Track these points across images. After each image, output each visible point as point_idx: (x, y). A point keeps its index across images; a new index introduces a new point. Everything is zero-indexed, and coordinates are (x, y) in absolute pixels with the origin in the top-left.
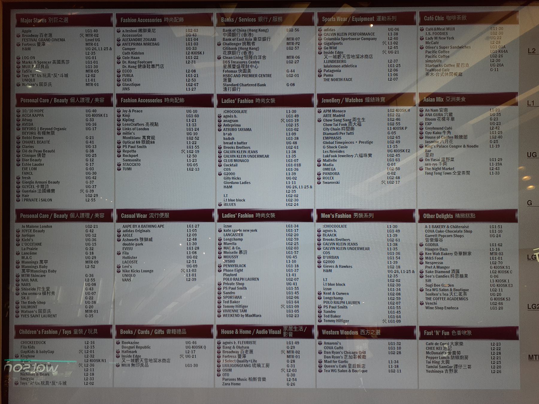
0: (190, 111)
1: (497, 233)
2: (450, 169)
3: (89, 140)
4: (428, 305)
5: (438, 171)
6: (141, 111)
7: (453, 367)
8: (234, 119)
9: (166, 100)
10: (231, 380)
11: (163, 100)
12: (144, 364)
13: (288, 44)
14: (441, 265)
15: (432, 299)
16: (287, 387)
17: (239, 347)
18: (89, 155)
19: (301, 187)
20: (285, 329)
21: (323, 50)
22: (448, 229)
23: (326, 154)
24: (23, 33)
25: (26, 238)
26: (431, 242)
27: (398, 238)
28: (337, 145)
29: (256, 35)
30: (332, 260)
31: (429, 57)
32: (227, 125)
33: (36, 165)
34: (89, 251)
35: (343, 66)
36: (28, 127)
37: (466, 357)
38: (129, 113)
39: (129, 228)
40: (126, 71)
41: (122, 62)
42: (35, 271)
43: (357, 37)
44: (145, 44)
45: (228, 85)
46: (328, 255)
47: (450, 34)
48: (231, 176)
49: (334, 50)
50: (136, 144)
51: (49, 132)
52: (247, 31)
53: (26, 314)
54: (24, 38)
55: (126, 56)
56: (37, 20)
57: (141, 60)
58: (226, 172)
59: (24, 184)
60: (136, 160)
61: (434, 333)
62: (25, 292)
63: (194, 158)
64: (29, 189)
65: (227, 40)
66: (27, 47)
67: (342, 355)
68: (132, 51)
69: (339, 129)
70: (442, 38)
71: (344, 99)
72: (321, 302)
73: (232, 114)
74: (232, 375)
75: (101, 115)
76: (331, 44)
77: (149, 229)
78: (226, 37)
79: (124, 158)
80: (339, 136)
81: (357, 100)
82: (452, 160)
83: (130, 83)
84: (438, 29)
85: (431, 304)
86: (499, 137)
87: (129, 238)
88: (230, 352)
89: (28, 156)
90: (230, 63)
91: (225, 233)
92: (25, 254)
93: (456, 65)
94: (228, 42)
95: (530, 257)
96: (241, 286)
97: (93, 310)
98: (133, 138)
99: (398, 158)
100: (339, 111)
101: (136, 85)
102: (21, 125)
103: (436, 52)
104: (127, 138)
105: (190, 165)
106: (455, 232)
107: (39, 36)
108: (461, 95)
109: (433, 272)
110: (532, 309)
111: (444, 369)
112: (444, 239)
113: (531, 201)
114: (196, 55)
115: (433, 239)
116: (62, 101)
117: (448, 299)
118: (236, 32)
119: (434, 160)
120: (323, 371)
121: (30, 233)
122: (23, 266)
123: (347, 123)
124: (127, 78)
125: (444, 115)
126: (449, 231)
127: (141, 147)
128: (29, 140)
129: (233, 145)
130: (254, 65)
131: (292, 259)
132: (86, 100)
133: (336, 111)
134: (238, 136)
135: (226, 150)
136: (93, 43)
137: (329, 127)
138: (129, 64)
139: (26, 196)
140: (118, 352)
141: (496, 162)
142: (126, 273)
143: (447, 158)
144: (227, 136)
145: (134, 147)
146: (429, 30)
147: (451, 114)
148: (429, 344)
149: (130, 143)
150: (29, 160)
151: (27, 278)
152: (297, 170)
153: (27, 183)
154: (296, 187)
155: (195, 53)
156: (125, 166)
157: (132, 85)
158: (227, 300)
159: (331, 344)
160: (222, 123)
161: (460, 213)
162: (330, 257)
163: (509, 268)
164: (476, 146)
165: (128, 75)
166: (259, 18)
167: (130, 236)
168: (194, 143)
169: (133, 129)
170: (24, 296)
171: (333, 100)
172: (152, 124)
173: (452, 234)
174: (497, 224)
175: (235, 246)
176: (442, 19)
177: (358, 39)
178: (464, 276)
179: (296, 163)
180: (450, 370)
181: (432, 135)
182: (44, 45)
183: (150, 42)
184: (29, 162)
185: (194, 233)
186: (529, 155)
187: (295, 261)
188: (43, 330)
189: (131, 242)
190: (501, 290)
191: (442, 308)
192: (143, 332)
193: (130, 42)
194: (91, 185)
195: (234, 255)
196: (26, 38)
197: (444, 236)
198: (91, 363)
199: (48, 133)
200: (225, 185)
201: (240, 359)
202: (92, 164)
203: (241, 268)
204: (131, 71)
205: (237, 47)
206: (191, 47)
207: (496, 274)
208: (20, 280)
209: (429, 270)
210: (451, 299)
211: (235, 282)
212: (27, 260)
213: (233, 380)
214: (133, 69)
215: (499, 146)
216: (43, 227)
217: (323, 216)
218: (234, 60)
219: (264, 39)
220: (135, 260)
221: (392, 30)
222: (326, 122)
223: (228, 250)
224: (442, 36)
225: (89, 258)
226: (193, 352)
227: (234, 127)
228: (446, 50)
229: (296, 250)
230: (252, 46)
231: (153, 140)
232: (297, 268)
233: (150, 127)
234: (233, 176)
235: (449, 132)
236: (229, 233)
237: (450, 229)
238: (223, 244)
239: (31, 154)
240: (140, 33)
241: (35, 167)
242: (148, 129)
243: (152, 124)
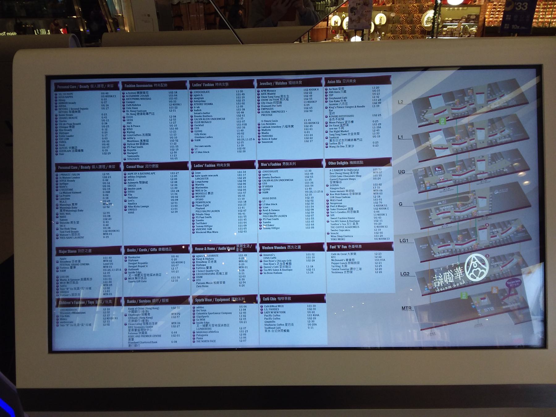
5: (338, 133)
20: (238, 246)
32: (197, 101)
37: (358, 263)
61: (337, 247)
67: (275, 263)
71: (275, 83)
80: (272, 107)
81: (283, 83)
96: (208, 216)
100: (271, 91)
111: (343, 271)
128: (63, 117)
129: (201, 115)
131: (242, 197)
133: (270, 91)
134: (204, 109)
137: (265, 102)
142: (131, 208)
159: (268, 255)
180: (348, 271)
187: (244, 199)
203: (208, 204)
211: (203, 213)
217: (262, 164)
227: (201, 103)
229: (245, 191)
232: (245, 203)
238: (195, 188)
239: (65, 126)
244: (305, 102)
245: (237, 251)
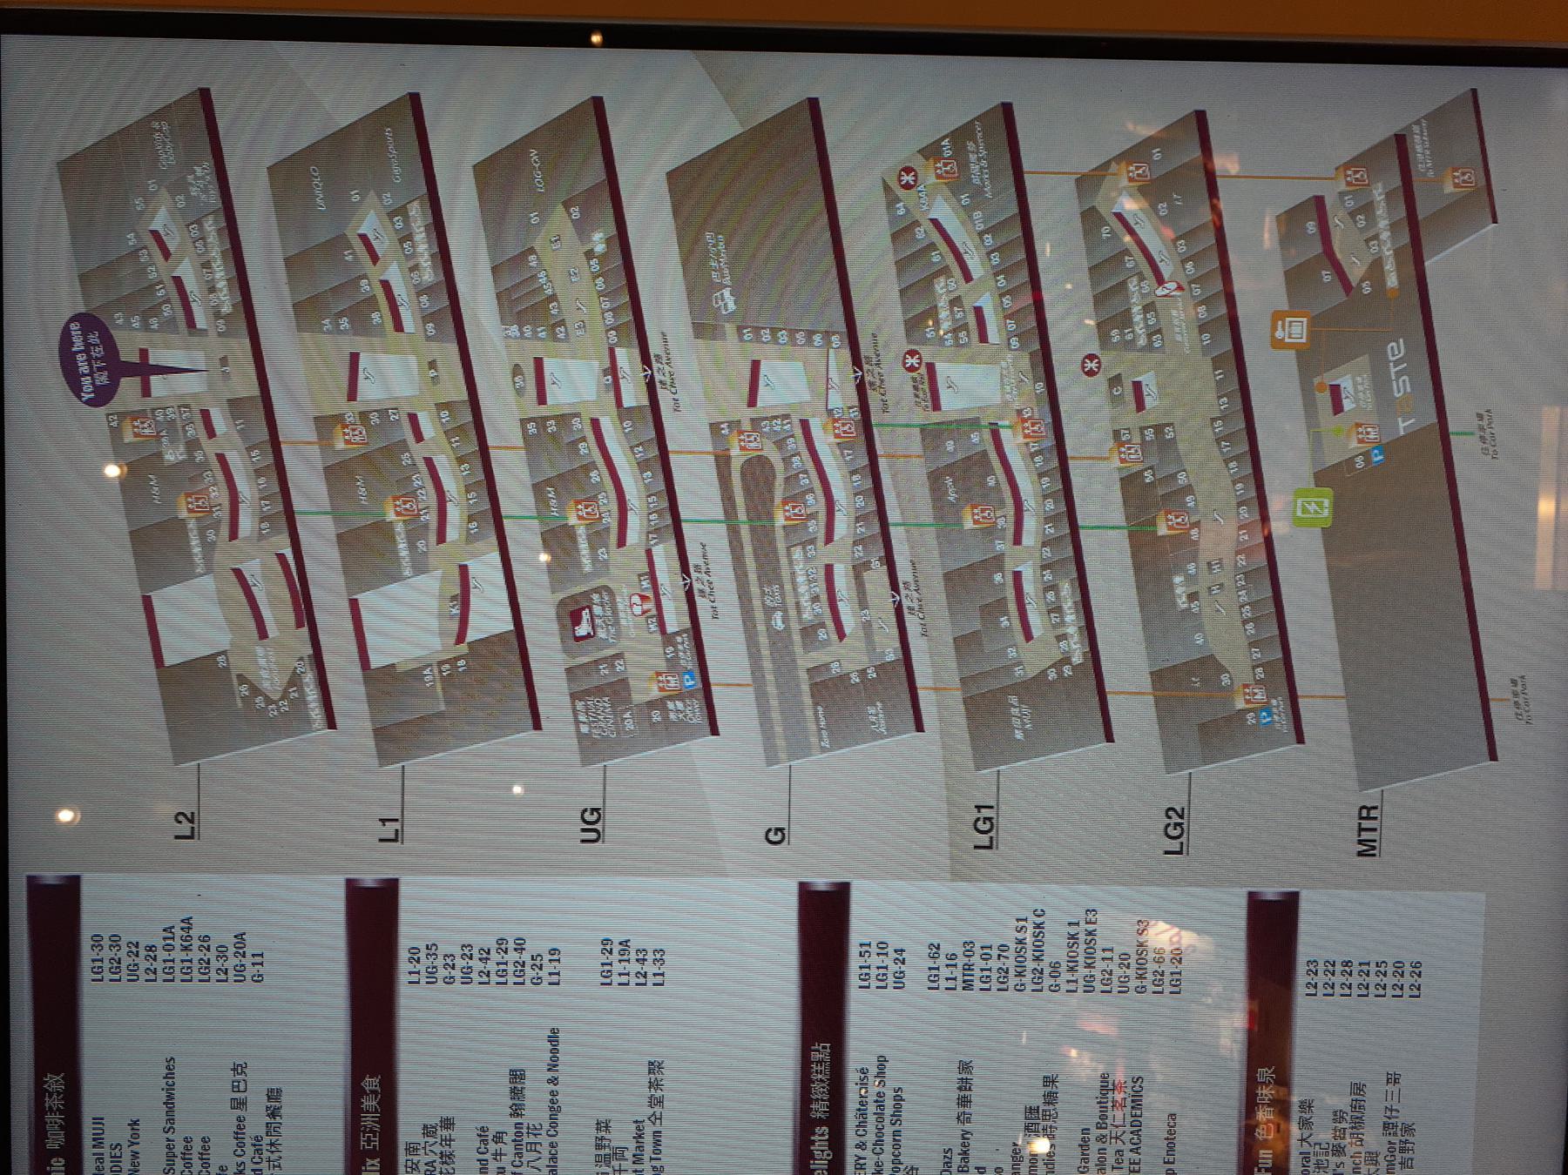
1: (888, 961)
2: (640, 1136)
22: (870, 1146)
47: (116, 1133)
70: (133, 1164)
82: (603, 1126)
86: (520, 949)
93: (238, 1112)
106: (880, 1117)
108: (356, 1092)
113: (770, 830)
117: (1136, 1151)
125: (431, 1157)
126: (879, 1142)
141: (616, 964)
143: (598, 1147)
147: (428, 1131)
163: (1026, 920)
173: (888, 1130)
174: (854, 962)
178: (1049, 1089)
180: (1402, 1150)
186: (593, 835)
190: (1108, 954)
207: (1047, 971)
210: (1135, 1141)
215: (553, 951)
228: (179, 1149)
235: (498, 1138)
237: (870, 1138)
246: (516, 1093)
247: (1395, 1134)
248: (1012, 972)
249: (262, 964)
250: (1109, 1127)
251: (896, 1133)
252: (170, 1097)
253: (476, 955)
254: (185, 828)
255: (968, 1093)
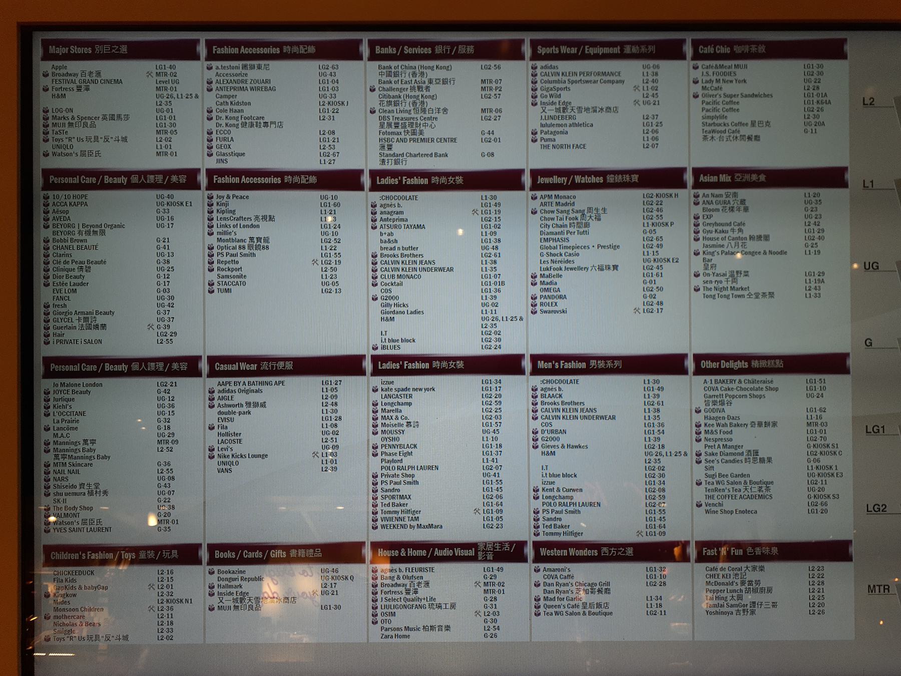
0: (325, 197)
1: (818, 391)
2: (742, 289)
3: (162, 244)
4: (708, 508)
5: (724, 293)
6: (247, 197)
7: (748, 606)
8: (397, 209)
9: (288, 179)
10: (395, 629)
11: (283, 180)
12: (255, 606)
13: (483, 89)
14: (729, 443)
15: (715, 498)
16: (485, 640)
17: (407, 577)
18: (162, 269)
19: (505, 319)
20: (481, 547)
21: (538, 100)
22: (739, 385)
23: (545, 266)
24: (54, 70)
25: (60, 403)
26: (714, 407)
27: (660, 399)
28: (563, 251)
29: (432, 75)
30: (556, 436)
31: (708, 111)
32: (386, 220)
33: (75, 284)
34: (162, 425)
35: (570, 126)
36: (61, 223)
37: (770, 590)
38: (227, 200)
39: (228, 387)
40: (221, 132)
41: (214, 118)
42: (75, 458)
43: (593, 78)
44: (252, 89)
45: (387, 156)
46: (549, 428)
47: (741, 74)
48: (392, 302)
49: (556, 100)
50: (238, 251)
51: (96, 232)
52: (417, 68)
53: (60, 526)
54: (55, 78)
55: (221, 107)
56: (76, 48)
57: (245, 114)
58: (385, 294)
59: (57, 316)
60: (238, 277)
62: (60, 491)
63: (334, 273)
64: (63, 324)
65: (384, 83)
66: (60, 93)
68: (231, 99)
69: (566, 226)
71: (574, 178)
72: (538, 504)
73: (393, 202)
74: (396, 622)
75: (182, 204)
76: (551, 89)
77: (261, 387)
78: (384, 78)
79: (219, 272)
80: (565, 236)
81: (593, 179)
83: (228, 151)
84: (722, 66)
85: (714, 505)
86: (820, 238)
87: (228, 402)
88: (393, 585)
89: (63, 270)
90: (391, 120)
91: (384, 393)
92: (58, 429)
93: (750, 124)
94: (386, 86)
95: (870, 430)
96: (410, 479)
97: (170, 519)
98: (233, 240)
99: (660, 271)
100: (564, 197)
101: (238, 155)
102: (51, 219)
103: (718, 103)
104: (224, 241)
105: (327, 284)
106: (751, 389)
107: (80, 75)
108: (758, 172)
109: (716, 454)
110: (873, 512)
111: (734, 610)
112: (734, 401)
114: (335, 107)
115: (716, 401)
116: (117, 180)
118: (400, 70)
119: (717, 275)
120: (542, 613)
121: (66, 396)
122: (55, 450)
123: (579, 215)
124: (223, 143)
125: (732, 203)
127: (245, 255)
128: (64, 244)
129: (396, 252)
130: (429, 122)
131: (492, 434)
132: (156, 178)
133: (561, 197)
134: (404, 237)
135: (384, 259)
136: (169, 86)
137: (550, 223)
138: (227, 121)
139: (59, 335)
140: (211, 587)
141: (814, 278)
142: (224, 460)
143: (737, 272)
144: (385, 237)
145: (236, 255)
146: (707, 67)
147: (743, 202)
148: (711, 570)
149: (228, 248)
150: (65, 277)
151: (63, 468)
152: (499, 291)
153: (60, 313)
154: (497, 319)
155: (333, 103)
156: (221, 287)
157: (232, 154)
158: (387, 501)
159: (554, 570)
160: (378, 216)
161: (758, 360)
162: (552, 432)
163: (837, 447)
164: (783, 253)
165: (225, 139)
166: (436, 47)
167: (230, 399)
168: (333, 248)
169: (234, 226)
170: (57, 497)
171: (556, 180)
172: (264, 218)
173: (747, 393)
175: (399, 415)
176: (727, 50)
177: (595, 82)
178: (766, 459)
179: (497, 280)
180: (744, 610)
181: (714, 235)
182: (87, 89)
183: (260, 85)
184: (65, 280)
185: (334, 393)
186: (867, 267)
188: (88, 552)
189: (230, 409)
190: (824, 482)
191: (732, 512)
192: (251, 555)
193: (228, 85)
194: (166, 317)
195: (398, 428)
196: (58, 78)
197: (733, 397)
198: (168, 605)
199: (95, 232)
200: (383, 316)
201: (408, 597)
202: (167, 283)
203: (410, 450)
204: (229, 132)
205: (402, 94)
206: (328, 94)
207: (817, 457)
208: (52, 472)
209: (709, 451)
210: (745, 497)
211: (399, 472)
212: (62, 440)
213: (398, 629)
214: (233, 129)
215: (819, 252)
216: (87, 385)
217: (541, 364)
218: (396, 115)
219: (445, 82)
220: (238, 438)
221: (648, 67)
222: (544, 215)
223: (387, 422)
224: (728, 78)
225: (163, 435)
226: (333, 585)
227: (398, 223)
228: (734, 99)
229: (498, 421)
230: (425, 93)
231: (266, 244)
232: (499, 450)
233: (261, 223)
234: (396, 301)
235: (740, 230)
236: (390, 393)
237: (743, 385)
238: (380, 411)
239: (67, 266)
240: (244, 71)
241: (74, 288)
242: (258, 226)
243: (264, 218)
244: (646, 225)
245: (480, 558)
246: (759, 238)
247: (751, 607)
248: (815, 442)
249: (812, 132)
250: (750, 486)
251: (746, 397)
252: (756, 96)
253: (817, 220)
254: (867, 101)
255: (764, 425)
